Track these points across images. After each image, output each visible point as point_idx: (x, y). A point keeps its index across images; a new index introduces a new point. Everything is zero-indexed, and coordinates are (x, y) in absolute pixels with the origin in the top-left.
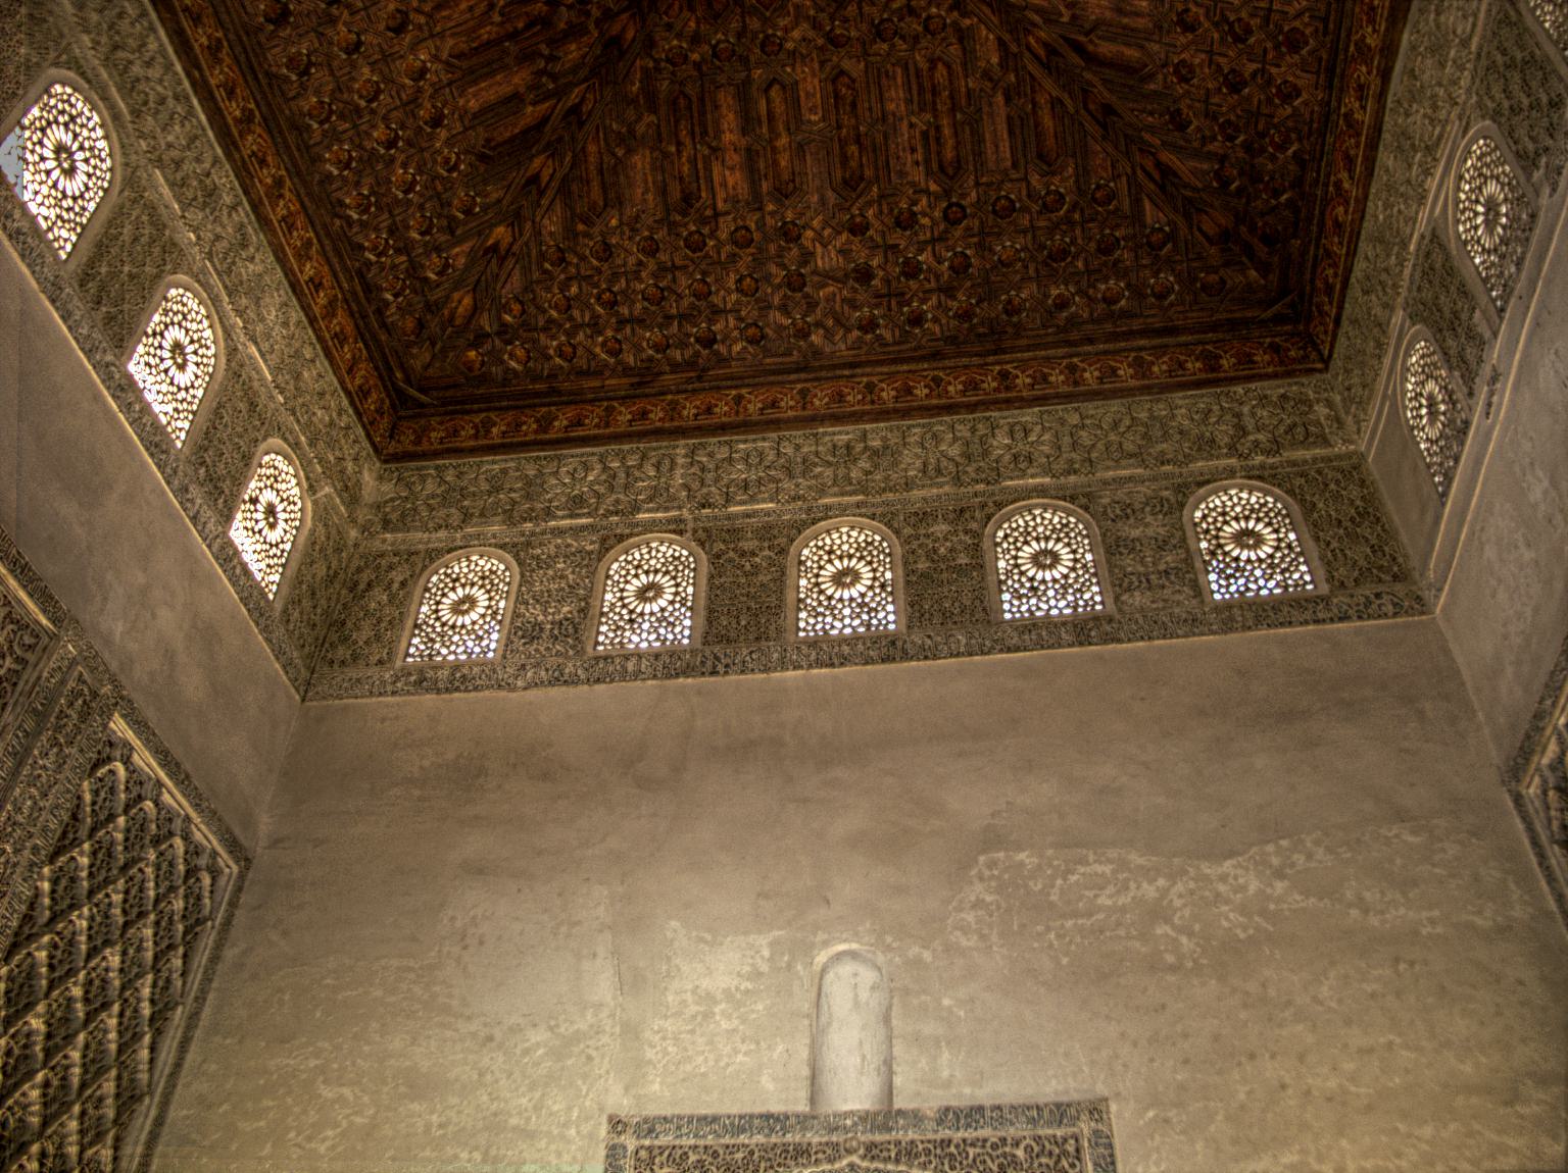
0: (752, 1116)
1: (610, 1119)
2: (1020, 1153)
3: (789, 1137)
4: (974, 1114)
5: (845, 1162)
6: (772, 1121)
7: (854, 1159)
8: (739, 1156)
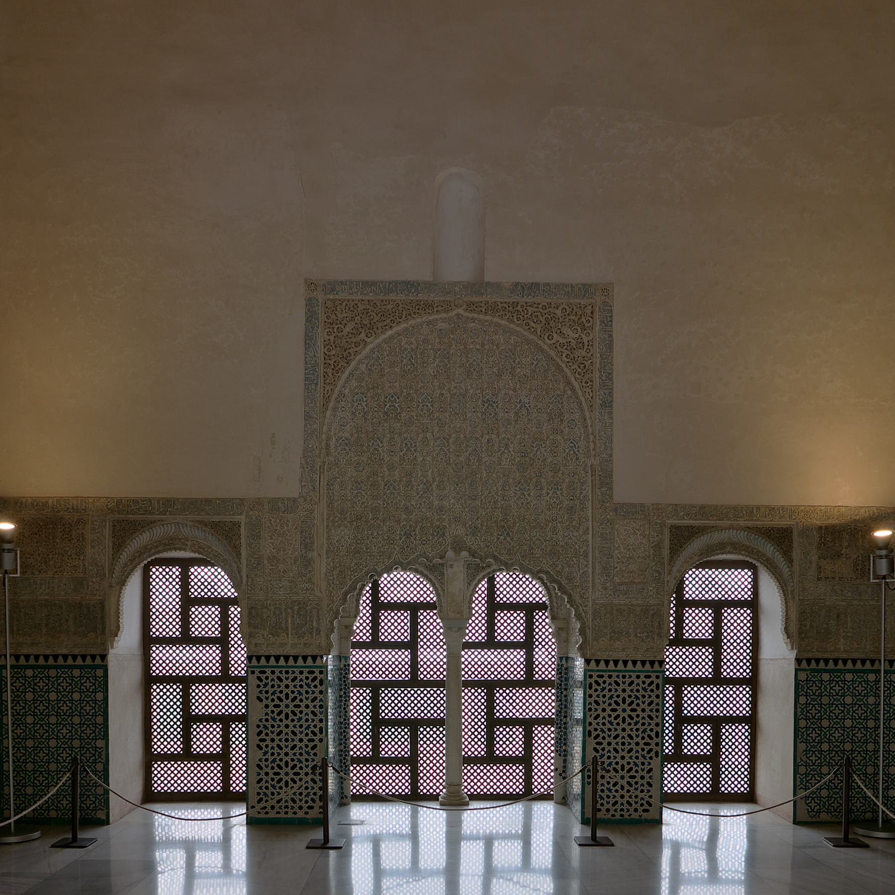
0: (396, 282)
1: (306, 280)
2: (558, 312)
3: (420, 296)
4: (533, 288)
5: (454, 312)
6: (409, 286)
7: (461, 311)
8: (389, 307)
